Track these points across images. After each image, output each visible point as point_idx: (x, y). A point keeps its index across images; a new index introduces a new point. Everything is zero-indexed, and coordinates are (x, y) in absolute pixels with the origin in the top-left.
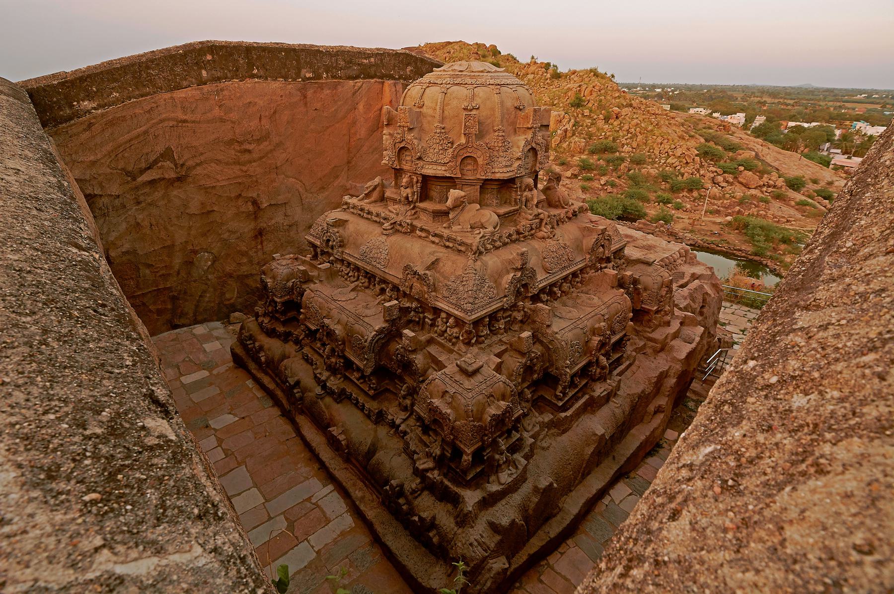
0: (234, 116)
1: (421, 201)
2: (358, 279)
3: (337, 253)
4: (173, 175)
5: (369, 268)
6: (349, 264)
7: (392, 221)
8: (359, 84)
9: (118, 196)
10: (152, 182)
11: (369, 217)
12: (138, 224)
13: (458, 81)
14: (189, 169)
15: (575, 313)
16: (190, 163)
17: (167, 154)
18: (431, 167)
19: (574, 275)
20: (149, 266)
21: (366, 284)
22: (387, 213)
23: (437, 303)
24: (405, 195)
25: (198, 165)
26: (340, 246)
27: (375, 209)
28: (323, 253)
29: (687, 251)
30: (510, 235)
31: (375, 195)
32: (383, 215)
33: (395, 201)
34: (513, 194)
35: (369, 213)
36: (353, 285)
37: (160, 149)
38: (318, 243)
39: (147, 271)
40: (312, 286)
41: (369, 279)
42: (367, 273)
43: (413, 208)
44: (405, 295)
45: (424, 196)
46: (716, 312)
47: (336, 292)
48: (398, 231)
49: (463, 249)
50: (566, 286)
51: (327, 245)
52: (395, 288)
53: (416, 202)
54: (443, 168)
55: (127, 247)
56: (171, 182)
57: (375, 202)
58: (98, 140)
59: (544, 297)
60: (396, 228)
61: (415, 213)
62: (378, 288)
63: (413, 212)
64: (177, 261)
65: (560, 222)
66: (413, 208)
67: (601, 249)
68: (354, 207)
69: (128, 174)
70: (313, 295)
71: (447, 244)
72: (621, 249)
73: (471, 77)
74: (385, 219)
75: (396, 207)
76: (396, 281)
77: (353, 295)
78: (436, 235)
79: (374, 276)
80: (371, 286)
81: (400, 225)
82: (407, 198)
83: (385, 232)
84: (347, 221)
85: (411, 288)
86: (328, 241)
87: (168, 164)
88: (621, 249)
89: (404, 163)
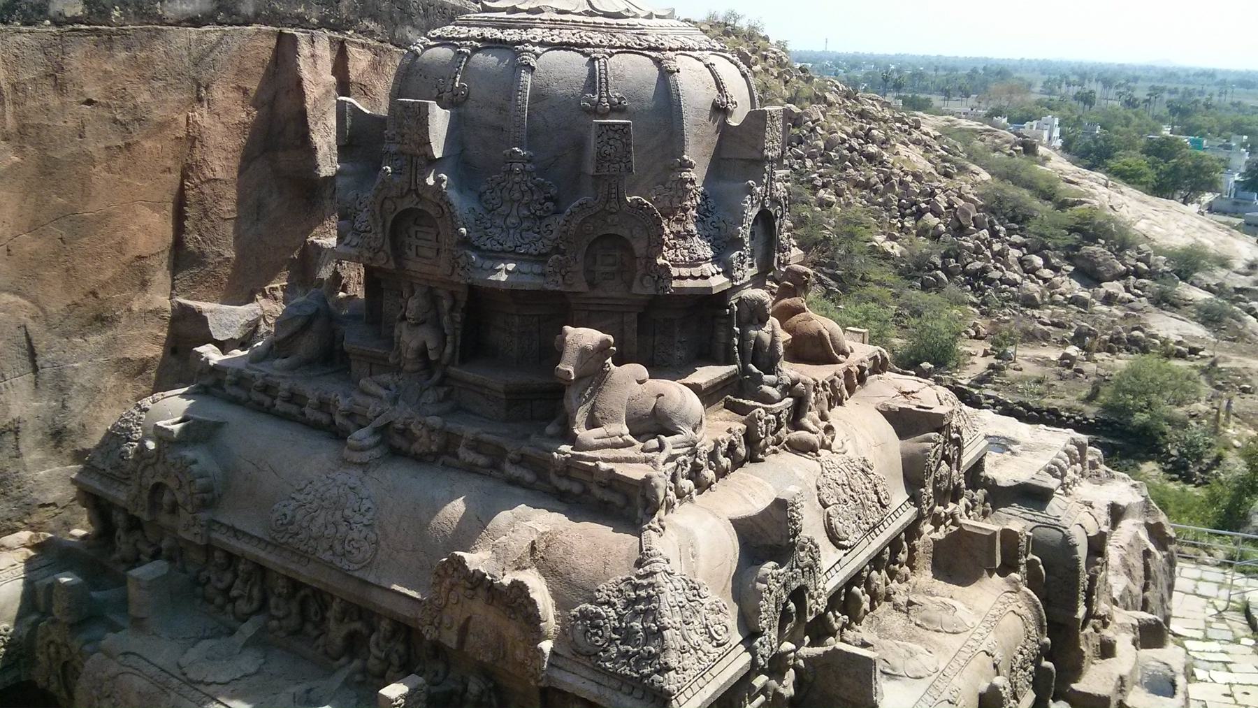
1: (463, 361)
2: (263, 607)
3: (187, 527)
5: (305, 573)
6: (232, 559)
7: (380, 422)
8: (213, 37)
11: (294, 409)
13: (566, 36)
15: (926, 661)
19: (894, 544)
21: (293, 622)
22: (360, 399)
23: (557, 674)
24: (414, 344)
26: (205, 505)
27: (312, 389)
28: (135, 524)
29: (1081, 447)
30: (732, 448)
31: (307, 345)
32: (343, 403)
33: (378, 364)
34: (722, 334)
35: (293, 398)
36: (248, 629)
38: (120, 495)
40: (110, 639)
41: (303, 604)
42: (295, 585)
43: (441, 384)
44: (438, 649)
45: (474, 345)
46: (1166, 596)
47: (193, 654)
48: (395, 453)
49: (617, 499)
50: (879, 578)
51: (154, 505)
52: (404, 631)
53: (451, 362)
54: (537, 268)
57: (309, 363)
59: (837, 620)
61: (447, 397)
62: (337, 633)
63: (442, 391)
65: (836, 400)
66: (441, 384)
67: (944, 467)
68: (241, 380)
70: (113, 668)
71: (564, 485)
72: (978, 465)
73: (596, 27)
74: (350, 415)
75: (386, 378)
76: (404, 611)
77: (248, 662)
78: (522, 461)
79: (321, 597)
80: (309, 627)
81: (405, 432)
82: (423, 352)
83: (357, 457)
84: (218, 425)
85: (464, 630)
86: (158, 488)
88: (978, 465)
89: (411, 254)
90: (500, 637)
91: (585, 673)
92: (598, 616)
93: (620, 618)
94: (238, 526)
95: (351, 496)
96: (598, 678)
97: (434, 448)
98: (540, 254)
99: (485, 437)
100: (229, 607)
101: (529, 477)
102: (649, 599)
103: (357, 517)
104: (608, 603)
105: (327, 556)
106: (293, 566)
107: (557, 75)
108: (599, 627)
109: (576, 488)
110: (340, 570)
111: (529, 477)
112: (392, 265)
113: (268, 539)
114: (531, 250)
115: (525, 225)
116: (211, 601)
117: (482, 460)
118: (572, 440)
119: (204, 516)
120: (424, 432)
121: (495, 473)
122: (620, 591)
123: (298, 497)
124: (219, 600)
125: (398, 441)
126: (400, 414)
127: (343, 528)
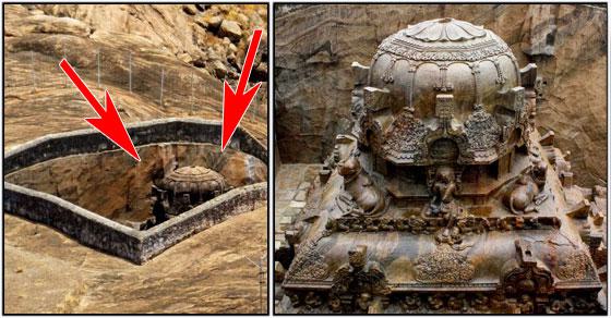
0: (378, 21)
4: (327, 60)
9: (294, 71)
10: (315, 64)
12: (305, 90)
14: (339, 57)
16: (341, 54)
17: (326, 46)
20: (309, 119)
25: (346, 55)
37: (322, 42)
39: (308, 122)
55: (296, 103)
56: (327, 66)
58: (288, 32)
64: (327, 120)
69: (301, 56)
87: (326, 53)
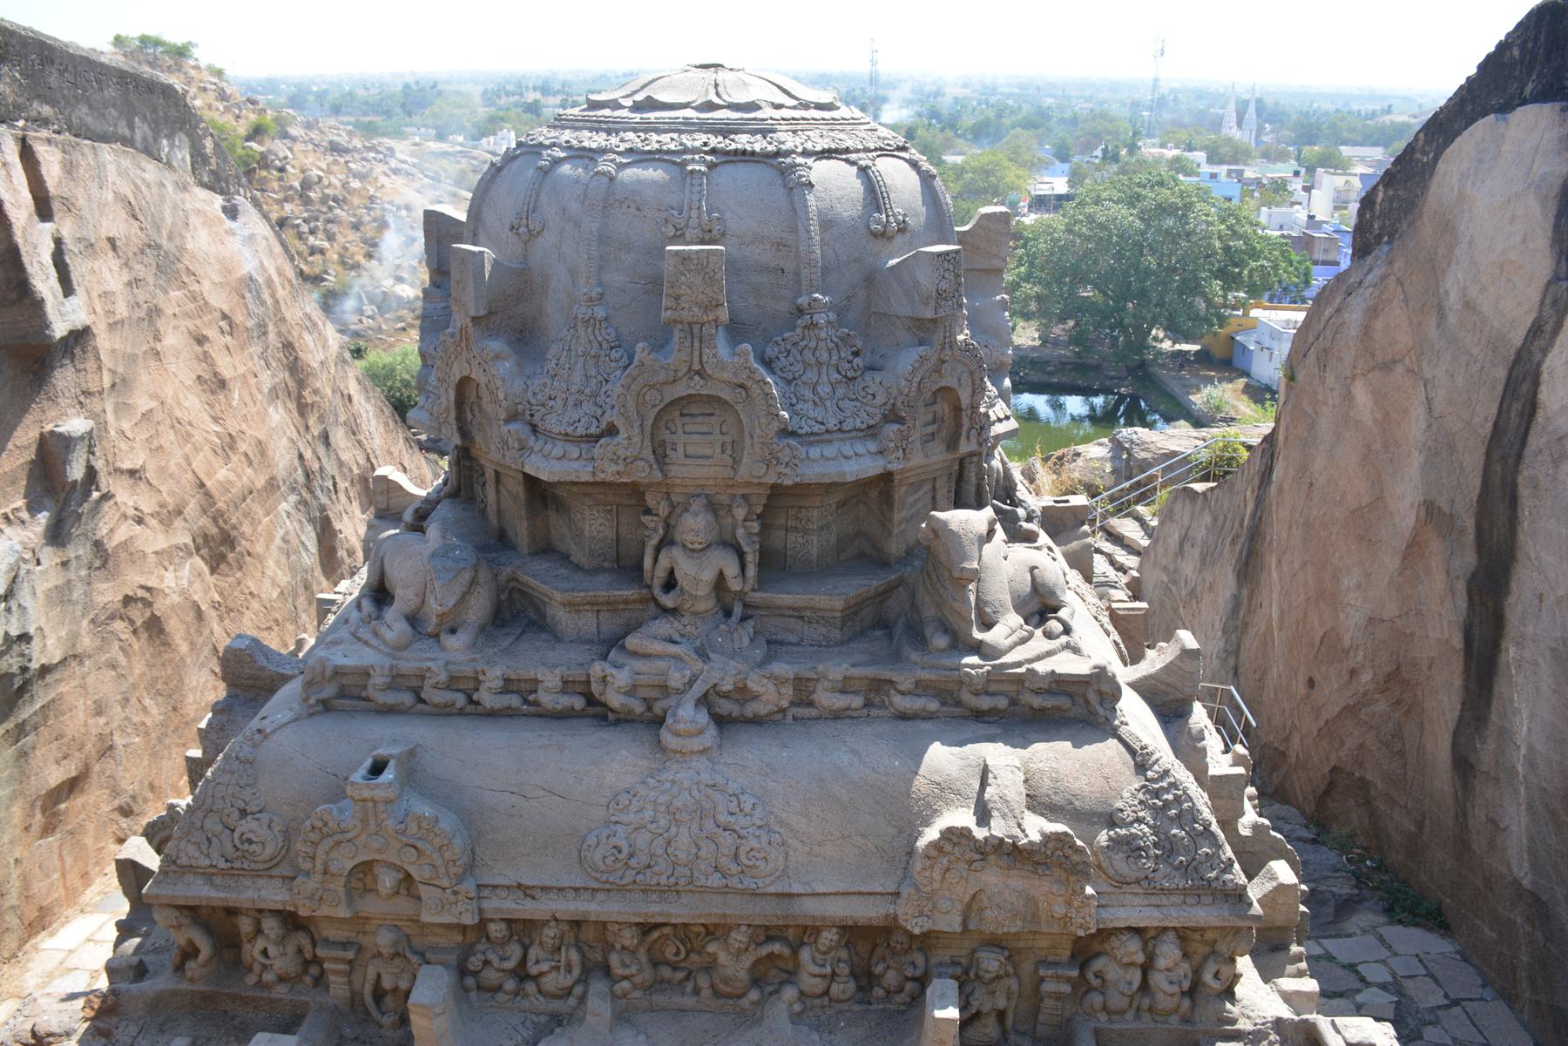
7: (699, 689)
18: (830, 451)
22: (639, 665)
24: (708, 575)
54: (872, 446)
60: (730, 717)
71: (985, 703)
82: (720, 581)
90: (1031, 901)
91: (1137, 900)
92: (1134, 837)
93: (1156, 830)
94: (526, 881)
95: (717, 796)
96: (1154, 900)
97: (785, 703)
98: (869, 427)
99: (855, 672)
100: (530, 987)
101: (933, 705)
102: (1177, 799)
103: (743, 821)
104: (1139, 820)
105: (716, 881)
106: (655, 908)
107: (838, 193)
108: (1140, 848)
109: (1002, 703)
110: (742, 892)
111: (933, 705)
112: (657, 475)
113: (595, 885)
114: (859, 425)
115: (841, 391)
116: (499, 988)
117: (857, 701)
118: (978, 648)
119: (469, 886)
120: (772, 688)
121: (874, 712)
122: (1141, 802)
123: (624, 818)
124: (510, 985)
125: (726, 707)
126: (723, 672)
127: (727, 840)
